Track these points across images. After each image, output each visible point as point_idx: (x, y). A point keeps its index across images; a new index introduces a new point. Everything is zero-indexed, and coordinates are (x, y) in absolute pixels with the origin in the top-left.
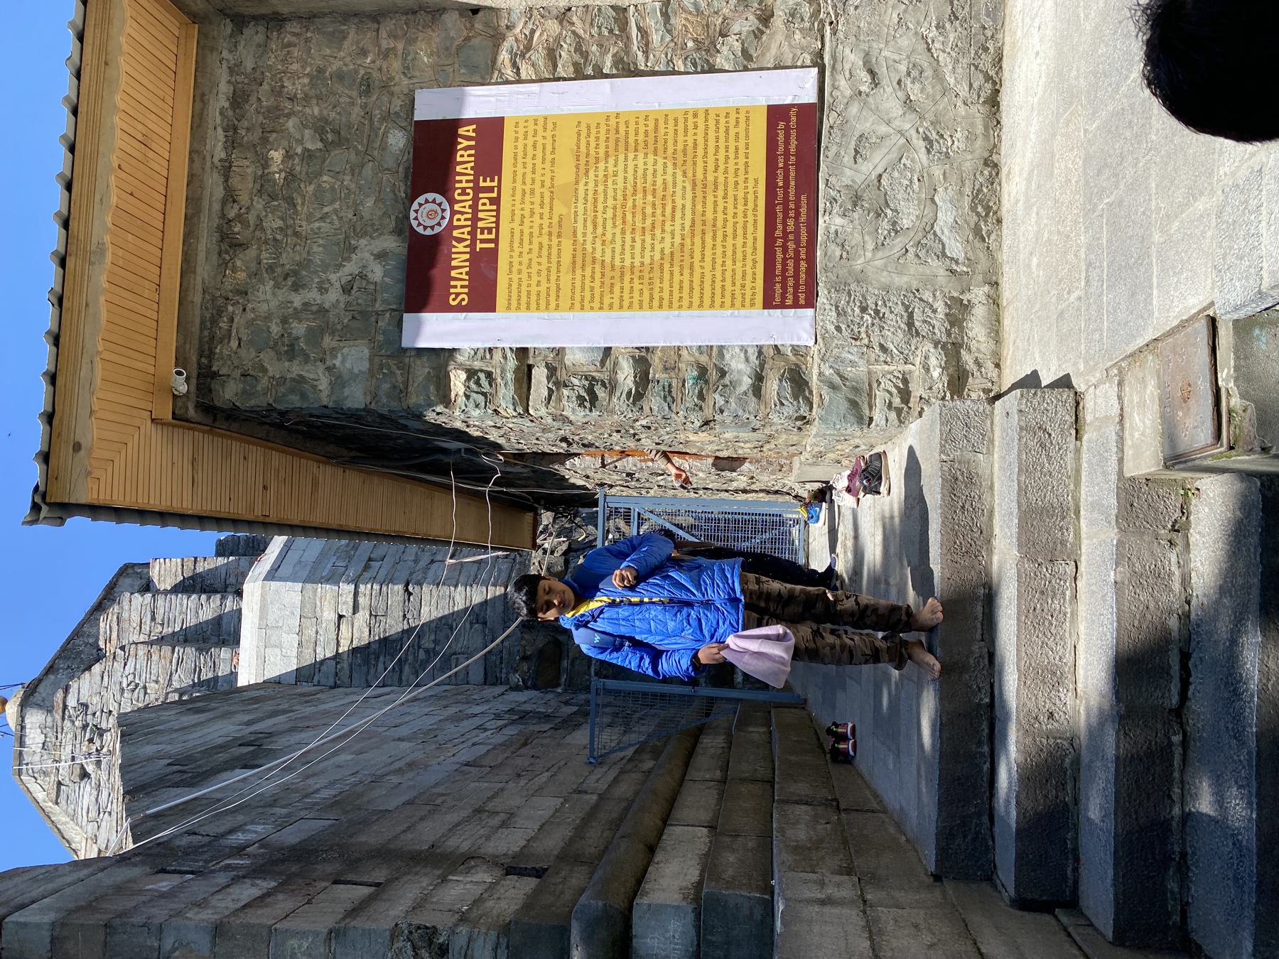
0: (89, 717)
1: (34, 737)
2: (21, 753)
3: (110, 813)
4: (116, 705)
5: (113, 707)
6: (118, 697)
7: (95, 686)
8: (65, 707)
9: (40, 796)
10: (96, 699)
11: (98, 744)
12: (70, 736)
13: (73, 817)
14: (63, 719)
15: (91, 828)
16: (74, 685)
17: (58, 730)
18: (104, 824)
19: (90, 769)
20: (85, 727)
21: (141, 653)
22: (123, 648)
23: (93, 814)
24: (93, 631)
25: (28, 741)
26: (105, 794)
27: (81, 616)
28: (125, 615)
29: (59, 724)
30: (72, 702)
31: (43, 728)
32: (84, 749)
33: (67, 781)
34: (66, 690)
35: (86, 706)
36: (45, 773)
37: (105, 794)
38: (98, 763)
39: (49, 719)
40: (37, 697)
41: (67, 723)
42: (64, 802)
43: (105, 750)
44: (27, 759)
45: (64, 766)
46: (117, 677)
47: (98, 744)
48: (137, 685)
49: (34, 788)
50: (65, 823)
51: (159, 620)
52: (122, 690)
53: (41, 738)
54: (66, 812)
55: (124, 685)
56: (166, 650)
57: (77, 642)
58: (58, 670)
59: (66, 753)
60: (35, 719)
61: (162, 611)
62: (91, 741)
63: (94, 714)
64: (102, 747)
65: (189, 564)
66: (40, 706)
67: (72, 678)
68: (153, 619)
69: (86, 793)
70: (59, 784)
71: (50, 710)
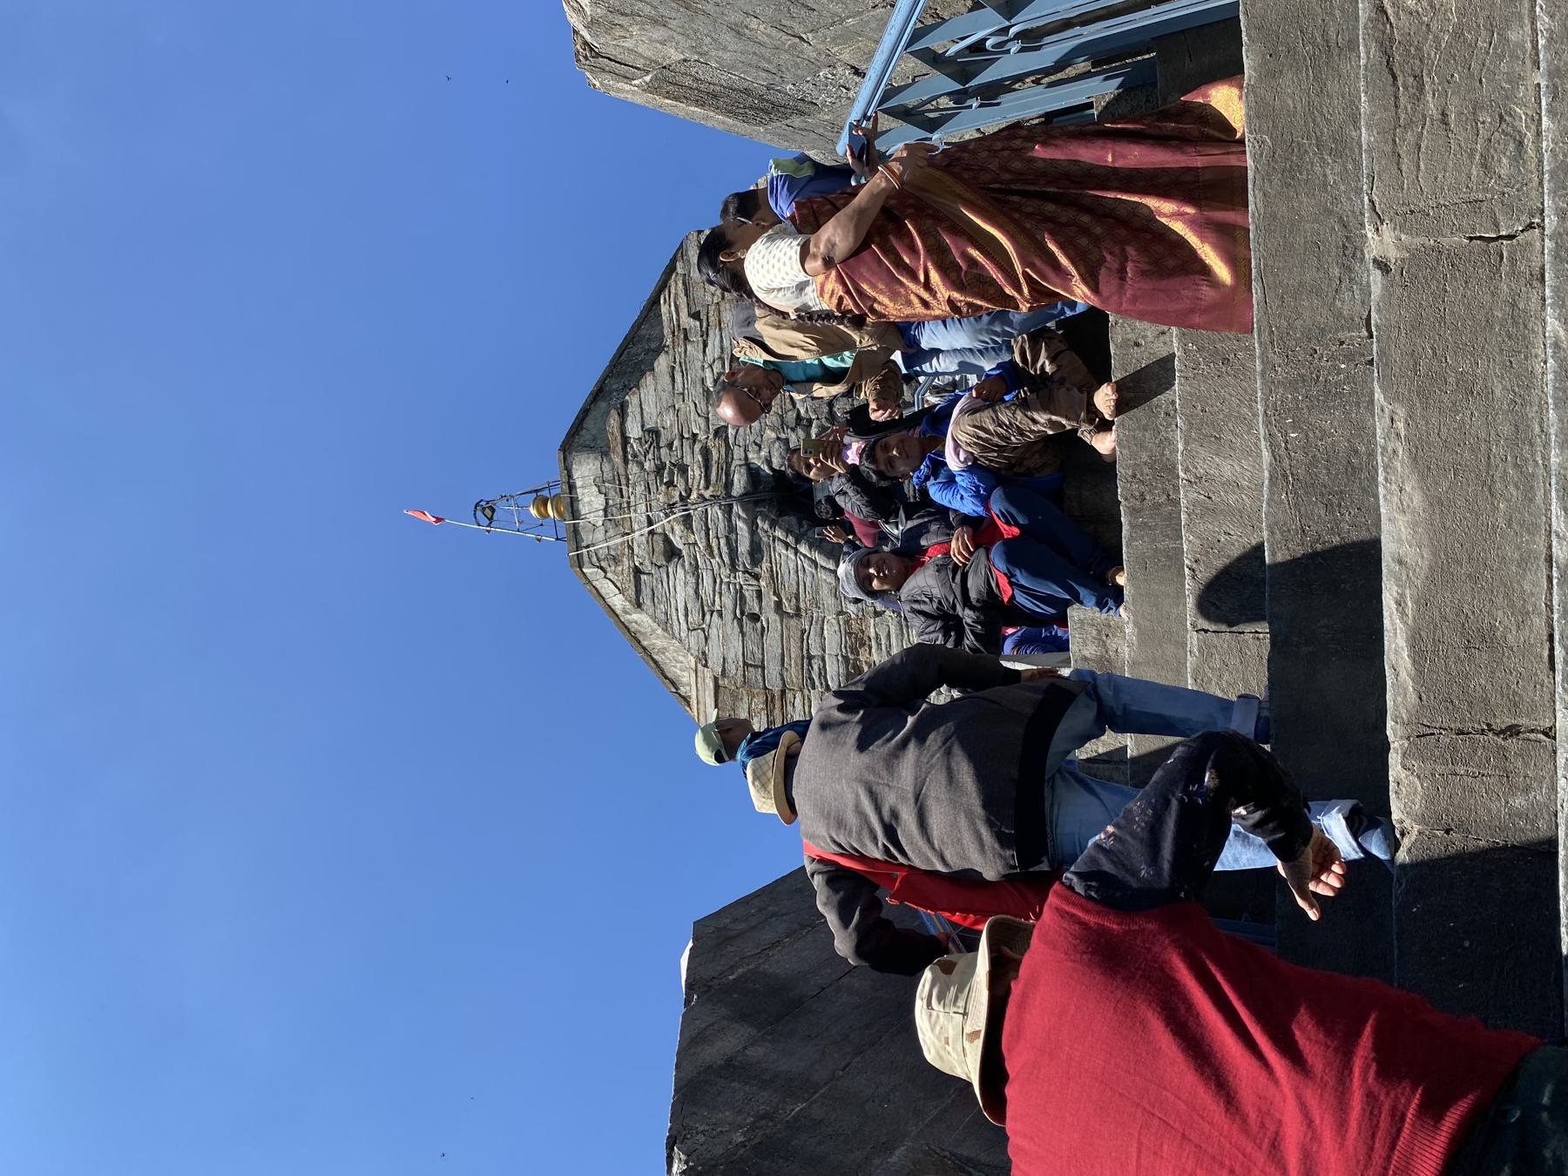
0: (663, 451)
1: (591, 501)
2: (576, 530)
3: (720, 614)
4: (701, 421)
6: (702, 406)
7: (665, 396)
8: (625, 441)
9: (618, 602)
10: (669, 419)
11: (681, 485)
12: (640, 489)
13: (666, 625)
14: (626, 461)
15: (695, 640)
16: (632, 400)
17: (620, 481)
18: (713, 632)
20: (659, 469)
21: (727, 316)
22: (696, 316)
23: (695, 617)
24: (655, 333)
25: (583, 509)
27: (635, 315)
29: (622, 471)
30: (634, 431)
31: (600, 484)
32: (662, 498)
33: (647, 567)
34: (623, 414)
35: (655, 433)
36: (616, 560)
38: (687, 521)
39: (607, 467)
40: (585, 436)
41: (633, 468)
42: (648, 602)
43: (694, 496)
44: (587, 538)
45: (639, 535)
47: (681, 485)
49: (607, 588)
50: (663, 651)
53: (599, 502)
54: (654, 618)
55: (709, 383)
57: (634, 350)
58: (611, 392)
59: (639, 515)
60: (586, 470)
62: (670, 484)
63: (670, 446)
64: (689, 491)
66: (590, 448)
67: (627, 388)
69: (679, 585)
70: (637, 572)
71: (605, 453)
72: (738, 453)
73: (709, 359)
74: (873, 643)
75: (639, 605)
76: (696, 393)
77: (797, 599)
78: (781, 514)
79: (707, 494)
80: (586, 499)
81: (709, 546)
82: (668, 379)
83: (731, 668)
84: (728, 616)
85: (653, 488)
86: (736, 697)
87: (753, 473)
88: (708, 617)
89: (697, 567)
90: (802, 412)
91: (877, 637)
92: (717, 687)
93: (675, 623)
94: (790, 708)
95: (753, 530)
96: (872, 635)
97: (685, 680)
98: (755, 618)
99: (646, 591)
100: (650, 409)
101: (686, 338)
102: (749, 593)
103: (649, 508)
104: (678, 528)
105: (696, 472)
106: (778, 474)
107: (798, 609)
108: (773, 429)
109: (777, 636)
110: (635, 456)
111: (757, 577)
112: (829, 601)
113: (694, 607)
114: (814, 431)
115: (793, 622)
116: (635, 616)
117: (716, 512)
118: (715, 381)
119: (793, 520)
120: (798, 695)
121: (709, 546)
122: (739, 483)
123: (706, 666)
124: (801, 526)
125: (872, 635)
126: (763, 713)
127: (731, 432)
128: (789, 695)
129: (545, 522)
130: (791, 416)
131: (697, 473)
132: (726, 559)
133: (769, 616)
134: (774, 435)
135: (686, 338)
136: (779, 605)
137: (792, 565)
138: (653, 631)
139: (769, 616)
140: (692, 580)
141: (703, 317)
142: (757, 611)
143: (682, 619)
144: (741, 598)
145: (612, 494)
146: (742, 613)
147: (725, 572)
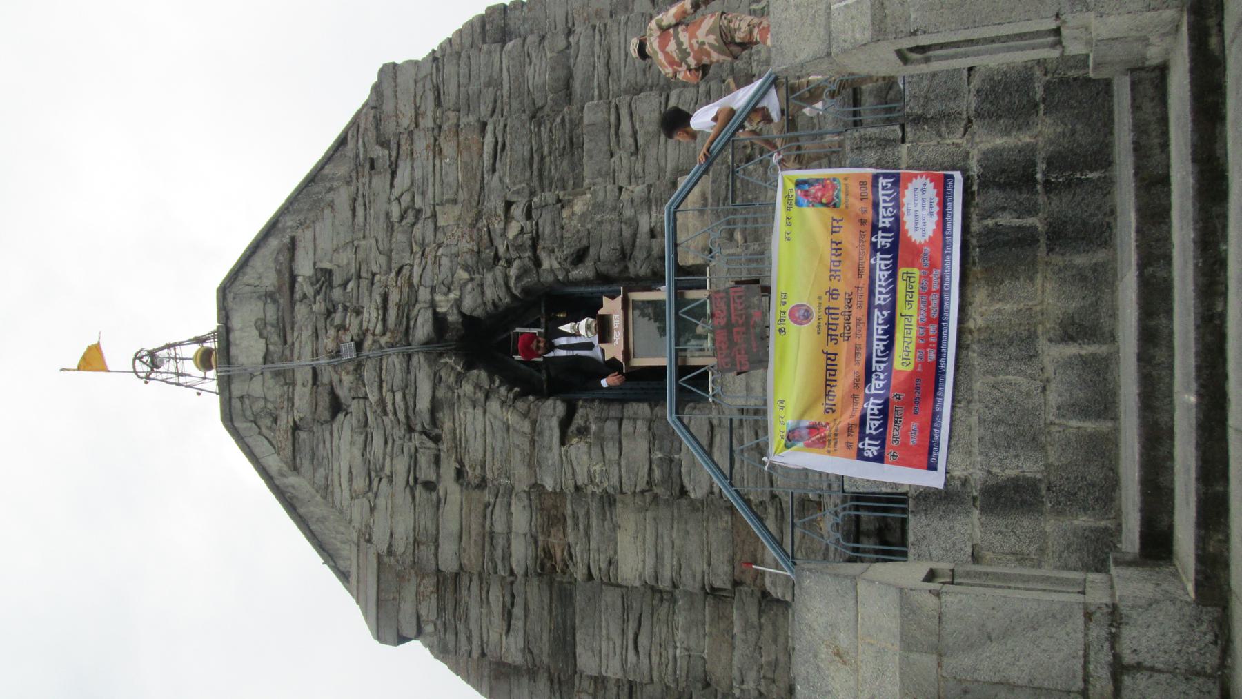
0: (337, 294)
4: (383, 260)
5: (377, 263)
10: (345, 257)
12: (307, 333)
18: (381, 502)
19: (345, 385)
22: (384, 144)
23: (360, 483)
26: (378, 440)
31: (261, 326)
37: (378, 440)
46: (380, 206)
48: (419, 211)
51: (449, 100)
52: (391, 228)
58: (284, 230)
62: (342, 328)
68: (438, 102)
72: (424, 294)
74: (569, 522)
75: (295, 469)
76: (379, 229)
77: (483, 467)
78: (469, 366)
80: (245, 343)
81: (382, 401)
82: (349, 214)
83: (400, 547)
84: (400, 480)
85: (321, 333)
86: (400, 577)
87: (439, 321)
88: (375, 483)
89: (366, 424)
90: (501, 250)
91: (575, 517)
92: (379, 563)
93: (337, 490)
94: (465, 592)
95: (437, 381)
96: (569, 512)
97: (345, 553)
98: (430, 486)
99: (305, 450)
100: (325, 244)
101: (372, 167)
102: (423, 460)
103: (316, 354)
104: (347, 379)
105: (371, 315)
106: (468, 321)
107: (484, 479)
108: (466, 268)
109: (456, 509)
110: (305, 296)
111: (437, 439)
113: (359, 471)
114: (513, 271)
115: (475, 494)
116: (292, 480)
117: (394, 361)
118: (402, 217)
119: (484, 375)
121: (382, 401)
122: (423, 329)
123: (369, 541)
124: (492, 381)
126: (434, 596)
127: (417, 270)
130: (488, 254)
131: (374, 314)
132: (402, 417)
133: (448, 484)
134: (465, 276)
135: (372, 167)
136: (460, 474)
137: (479, 427)
138: (313, 497)
139: (448, 484)
140: (360, 439)
141: (393, 146)
142: (433, 478)
143: (345, 485)
144: (414, 463)
145: (275, 338)
146: (416, 479)
147: (399, 432)
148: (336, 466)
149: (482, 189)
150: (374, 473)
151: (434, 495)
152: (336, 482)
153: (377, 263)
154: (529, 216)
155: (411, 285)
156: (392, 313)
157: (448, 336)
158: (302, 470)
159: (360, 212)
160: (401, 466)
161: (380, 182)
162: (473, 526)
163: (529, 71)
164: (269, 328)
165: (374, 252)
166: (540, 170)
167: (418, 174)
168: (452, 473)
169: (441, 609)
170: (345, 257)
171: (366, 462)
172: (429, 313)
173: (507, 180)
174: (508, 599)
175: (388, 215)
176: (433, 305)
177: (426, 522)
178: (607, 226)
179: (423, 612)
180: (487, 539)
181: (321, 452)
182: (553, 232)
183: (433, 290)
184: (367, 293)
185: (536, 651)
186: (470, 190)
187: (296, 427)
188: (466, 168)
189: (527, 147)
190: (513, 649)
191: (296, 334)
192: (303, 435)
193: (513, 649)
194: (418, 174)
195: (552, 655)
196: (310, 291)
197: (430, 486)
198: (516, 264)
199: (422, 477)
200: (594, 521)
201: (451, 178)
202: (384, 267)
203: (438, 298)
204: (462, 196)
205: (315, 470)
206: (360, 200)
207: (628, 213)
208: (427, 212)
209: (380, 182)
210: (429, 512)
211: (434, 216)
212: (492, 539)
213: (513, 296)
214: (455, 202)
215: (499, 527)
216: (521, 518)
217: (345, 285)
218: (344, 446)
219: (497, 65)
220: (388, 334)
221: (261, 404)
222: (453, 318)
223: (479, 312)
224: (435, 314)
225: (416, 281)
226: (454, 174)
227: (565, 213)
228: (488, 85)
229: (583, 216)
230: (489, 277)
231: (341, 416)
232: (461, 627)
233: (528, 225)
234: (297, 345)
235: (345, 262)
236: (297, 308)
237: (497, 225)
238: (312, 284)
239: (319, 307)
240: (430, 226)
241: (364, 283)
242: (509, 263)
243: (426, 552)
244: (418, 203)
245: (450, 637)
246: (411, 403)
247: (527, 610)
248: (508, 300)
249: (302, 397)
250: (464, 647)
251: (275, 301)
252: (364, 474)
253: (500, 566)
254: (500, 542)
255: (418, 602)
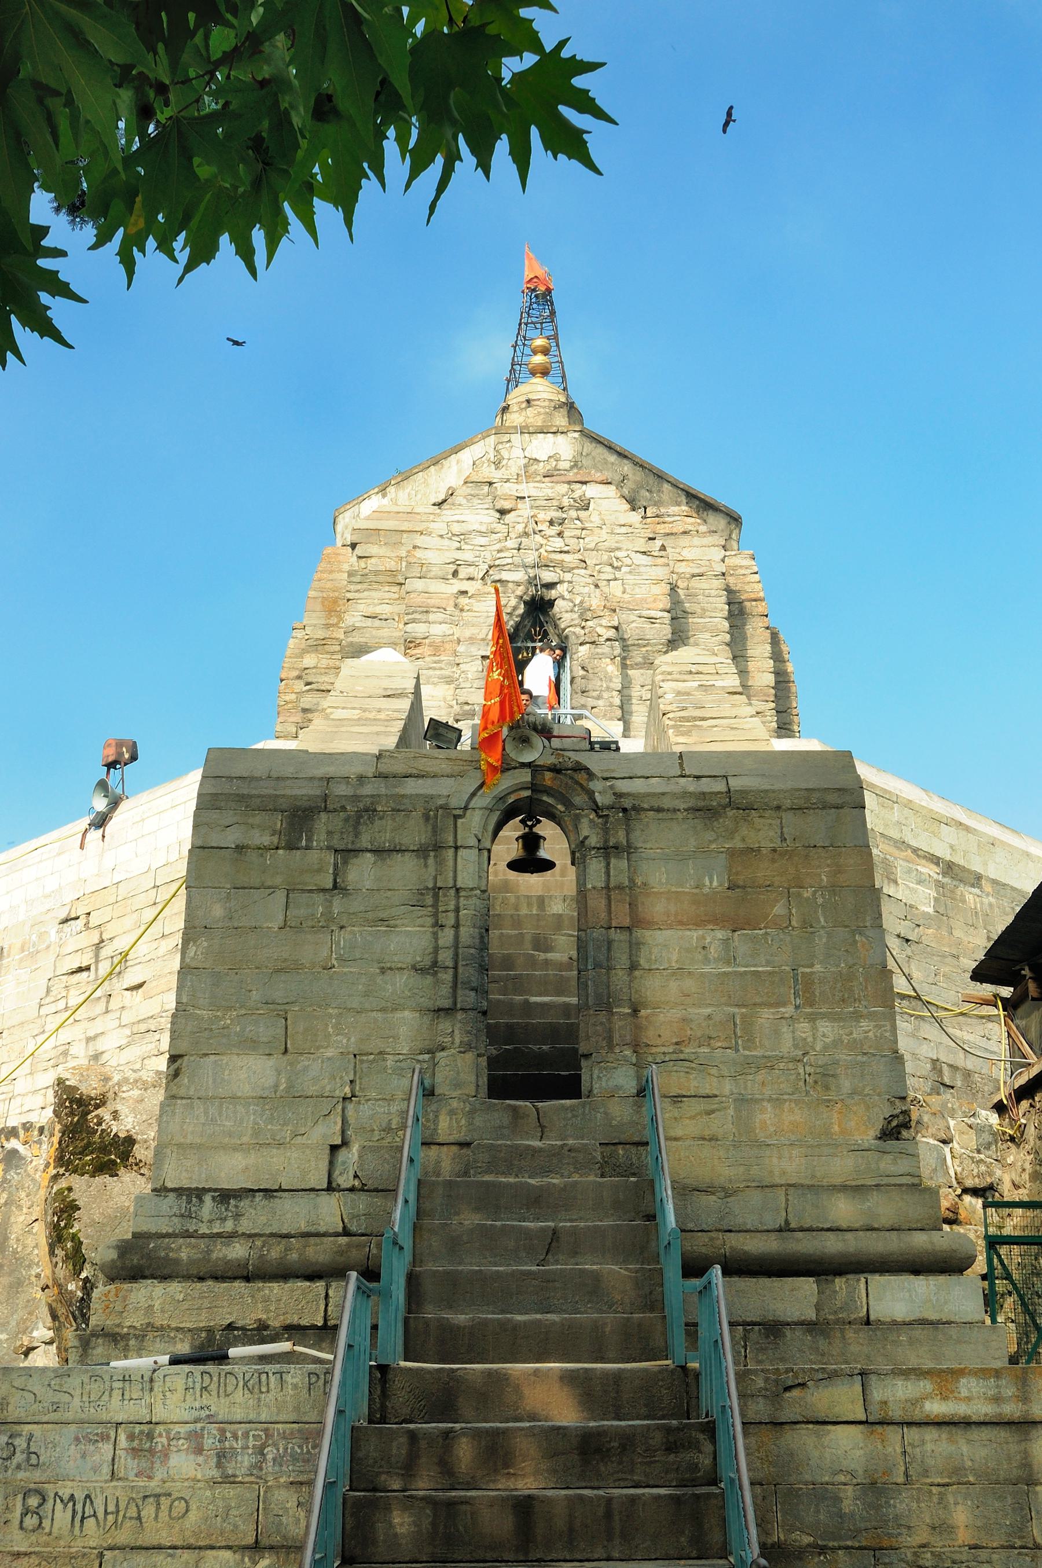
0: (573, 514)
4: (592, 545)
5: (590, 541)
10: (596, 519)
12: (550, 493)
14: (569, 483)
18: (446, 542)
23: (456, 528)
26: (483, 541)
28: (696, 541)
30: (591, 491)
31: (555, 457)
37: (483, 541)
51: (695, 583)
55: (618, 554)
56: (665, 602)
61: (705, 586)
65: (761, 608)
71: (575, 465)
72: (568, 576)
73: (633, 555)
74: (437, 658)
79: (542, 550)
83: (418, 553)
84: (459, 555)
94: (387, 589)
95: (518, 584)
96: (442, 658)
98: (455, 574)
101: (650, 539)
102: (471, 569)
106: (551, 603)
108: (582, 602)
112: (468, 633)
115: (452, 603)
120: (396, 596)
122: (548, 576)
125: (442, 658)
127: (582, 572)
128: (396, 589)
129: (527, 351)
130: (589, 615)
132: (497, 562)
133: (458, 585)
134: (577, 602)
135: (650, 539)
136: (464, 593)
139: (458, 585)
142: (461, 576)
143: (456, 518)
148: (467, 512)
149: (631, 610)
150: (463, 537)
151: (451, 577)
152: (457, 512)
153: (590, 541)
154: (608, 640)
155: (573, 568)
156: (559, 557)
157: (544, 590)
158: (464, 488)
159: (624, 530)
160: (467, 556)
161: (641, 544)
162: (433, 601)
163: (707, 635)
164: (554, 463)
165: (597, 540)
166: (638, 645)
167: (642, 569)
168: (463, 589)
169: (377, 573)
170: (596, 519)
171: (470, 533)
172: (556, 580)
173: (634, 625)
174: (384, 616)
175: (618, 549)
176: (561, 582)
177: (435, 571)
178: (599, 683)
179: (373, 560)
180: (425, 609)
181: (476, 501)
182: (598, 654)
183: (570, 582)
184: (572, 534)
185: (354, 633)
186: (629, 602)
187: (491, 484)
188: (645, 600)
189: (651, 637)
190: (354, 619)
191: (550, 485)
192: (486, 488)
193: (354, 619)
194: (642, 569)
195: (351, 644)
196: (576, 495)
197: (455, 574)
198: (583, 632)
199: (461, 569)
200: (438, 672)
201: (637, 590)
202: (588, 546)
203: (566, 584)
204: (626, 596)
205: (465, 497)
206: (630, 530)
207: (605, 695)
208: (618, 575)
209: (641, 544)
210: (440, 574)
211: (616, 579)
212: (426, 612)
213: (564, 630)
214: (624, 592)
215: (432, 617)
216: (437, 630)
217: (578, 519)
218: (477, 516)
219: (714, 614)
220: (546, 554)
221: (506, 456)
222: (553, 594)
223: (556, 609)
224: (557, 583)
225: (575, 571)
226: (640, 592)
227: (608, 660)
228: (703, 609)
229: (606, 672)
230: (576, 616)
231: (498, 515)
232: (365, 586)
233: (602, 639)
234: (543, 485)
235: (592, 519)
236: (566, 485)
237: (604, 622)
238: (580, 497)
239: (566, 502)
240: (611, 577)
241: (578, 533)
242: (583, 628)
243: (416, 571)
244: (624, 569)
245: (358, 579)
246: (506, 568)
247: (378, 628)
248: (563, 626)
249: (512, 489)
250: (352, 587)
251: (572, 467)
252: (463, 531)
253: (410, 617)
254: (423, 617)
255: (380, 557)
